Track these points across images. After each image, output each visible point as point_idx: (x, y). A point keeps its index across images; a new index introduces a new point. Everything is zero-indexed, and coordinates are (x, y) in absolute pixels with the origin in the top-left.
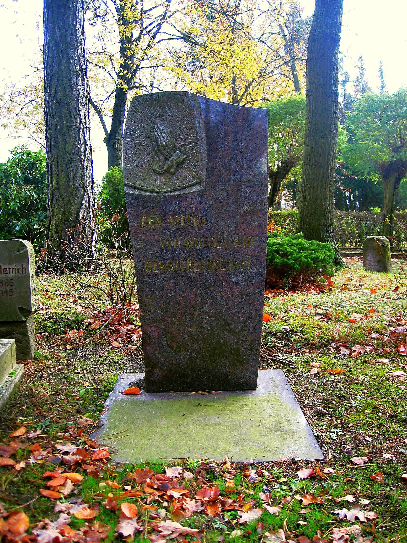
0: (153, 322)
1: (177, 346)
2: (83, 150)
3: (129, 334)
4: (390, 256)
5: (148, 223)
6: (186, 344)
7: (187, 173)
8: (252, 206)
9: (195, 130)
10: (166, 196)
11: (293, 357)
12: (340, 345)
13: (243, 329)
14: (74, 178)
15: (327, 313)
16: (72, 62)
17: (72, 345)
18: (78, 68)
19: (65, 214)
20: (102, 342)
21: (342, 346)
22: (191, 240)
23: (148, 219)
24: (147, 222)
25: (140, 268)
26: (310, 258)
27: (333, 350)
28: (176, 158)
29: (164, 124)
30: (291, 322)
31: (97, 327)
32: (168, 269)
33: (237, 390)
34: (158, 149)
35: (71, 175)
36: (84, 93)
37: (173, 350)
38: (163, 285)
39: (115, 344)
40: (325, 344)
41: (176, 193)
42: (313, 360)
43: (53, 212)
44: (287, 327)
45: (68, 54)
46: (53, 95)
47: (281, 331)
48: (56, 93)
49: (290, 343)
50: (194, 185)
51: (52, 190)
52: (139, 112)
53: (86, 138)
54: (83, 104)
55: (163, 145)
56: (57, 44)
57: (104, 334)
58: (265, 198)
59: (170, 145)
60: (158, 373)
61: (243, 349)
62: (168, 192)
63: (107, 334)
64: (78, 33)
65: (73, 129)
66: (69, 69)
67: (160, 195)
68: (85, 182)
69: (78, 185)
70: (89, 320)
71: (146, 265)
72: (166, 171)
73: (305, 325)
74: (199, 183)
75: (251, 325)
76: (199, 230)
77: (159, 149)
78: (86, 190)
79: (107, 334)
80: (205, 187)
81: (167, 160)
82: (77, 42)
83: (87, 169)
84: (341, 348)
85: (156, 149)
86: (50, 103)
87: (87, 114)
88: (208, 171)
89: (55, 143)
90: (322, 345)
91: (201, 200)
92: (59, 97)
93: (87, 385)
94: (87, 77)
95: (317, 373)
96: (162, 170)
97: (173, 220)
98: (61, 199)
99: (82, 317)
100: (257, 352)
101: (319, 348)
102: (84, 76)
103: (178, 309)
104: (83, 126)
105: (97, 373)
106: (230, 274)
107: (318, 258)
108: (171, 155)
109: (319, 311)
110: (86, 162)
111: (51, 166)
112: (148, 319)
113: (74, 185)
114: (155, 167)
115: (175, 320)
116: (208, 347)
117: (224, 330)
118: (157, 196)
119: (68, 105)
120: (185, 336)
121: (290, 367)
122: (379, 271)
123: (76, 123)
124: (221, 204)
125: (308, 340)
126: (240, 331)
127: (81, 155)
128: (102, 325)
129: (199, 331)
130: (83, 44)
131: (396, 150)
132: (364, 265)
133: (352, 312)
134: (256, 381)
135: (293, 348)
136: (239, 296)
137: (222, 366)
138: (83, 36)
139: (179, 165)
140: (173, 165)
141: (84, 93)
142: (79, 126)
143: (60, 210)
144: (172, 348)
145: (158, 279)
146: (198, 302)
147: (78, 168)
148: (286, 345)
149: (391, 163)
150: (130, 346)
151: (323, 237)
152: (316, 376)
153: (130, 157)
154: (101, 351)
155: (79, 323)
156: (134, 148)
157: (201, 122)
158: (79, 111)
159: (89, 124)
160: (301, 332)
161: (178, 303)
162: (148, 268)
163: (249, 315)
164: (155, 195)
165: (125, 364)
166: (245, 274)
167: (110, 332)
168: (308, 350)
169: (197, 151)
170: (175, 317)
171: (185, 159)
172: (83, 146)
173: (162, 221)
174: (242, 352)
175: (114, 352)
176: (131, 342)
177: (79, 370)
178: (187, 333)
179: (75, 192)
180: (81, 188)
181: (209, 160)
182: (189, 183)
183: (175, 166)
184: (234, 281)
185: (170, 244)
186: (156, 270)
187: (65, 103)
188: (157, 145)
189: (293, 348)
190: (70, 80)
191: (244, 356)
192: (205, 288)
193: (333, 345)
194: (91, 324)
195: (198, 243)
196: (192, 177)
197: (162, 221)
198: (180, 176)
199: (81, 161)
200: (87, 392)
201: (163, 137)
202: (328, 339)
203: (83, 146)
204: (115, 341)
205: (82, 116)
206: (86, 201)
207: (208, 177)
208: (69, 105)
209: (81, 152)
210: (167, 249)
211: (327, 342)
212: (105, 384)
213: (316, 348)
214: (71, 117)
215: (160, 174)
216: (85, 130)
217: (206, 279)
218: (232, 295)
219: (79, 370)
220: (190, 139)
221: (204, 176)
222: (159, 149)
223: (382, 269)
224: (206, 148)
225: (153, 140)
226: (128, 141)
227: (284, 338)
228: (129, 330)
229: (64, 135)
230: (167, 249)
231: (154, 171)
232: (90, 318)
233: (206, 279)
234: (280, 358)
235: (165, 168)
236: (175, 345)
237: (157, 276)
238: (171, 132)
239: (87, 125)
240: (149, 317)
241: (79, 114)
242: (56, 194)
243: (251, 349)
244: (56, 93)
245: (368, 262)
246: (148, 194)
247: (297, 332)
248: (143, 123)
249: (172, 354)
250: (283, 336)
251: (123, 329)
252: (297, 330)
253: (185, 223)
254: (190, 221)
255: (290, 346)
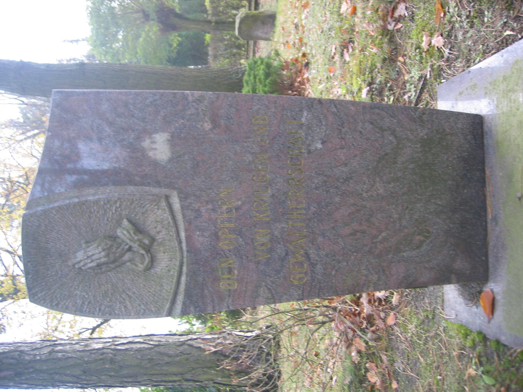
0: (384, 271)
1: (419, 234)
2: (139, 346)
3: (375, 301)
4: (257, 12)
5: (229, 279)
6: (417, 220)
7: (152, 218)
8: (204, 115)
9: (84, 204)
10: (188, 251)
11: (412, 77)
12: (392, 17)
13: (393, 133)
14: (170, 356)
15: (340, 46)
16: (38, 358)
17: (390, 379)
18: (46, 351)
19: (211, 367)
20: (386, 339)
21: (393, 14)
22: (257, 212)
23: (223, 279)
24: (228, 282)
25: (300, 292)
26: (265, 82)
27: (399, 26)
28: (128, 235)
29: (75, 253)
30: (355, 88)
31: (364, 344)
32: (302, 248)
33: (483, 143)
34: (114, 262)
35: (166, 359)
36: (75, 344)
37: (424, 241)
38: (327, 255)
39: (391, 321)
40: (391, 38)
41: (183, 235)
42: (419, 47)
43: (208, 380)
44: (365, 91)
45: (30, 362)
46: (75, 380)
47: (371, 97)
48: (74, 376)
49: (389, 85)
50: (170, 206)
51: (183, 381)
52: (54, 292)
53: (125, 342)
54: (86, 346)
55: (107, 255)
56: (18, 374)
57: (375, 336)
58: (192, 95)
59: (106, 244)
60: (460, 264)
61: (423, 133)
62: (181, 249)
63: (373, 332)
64: (6, 350)
65: (115, 357)
66: (46, 361)
67: (185, 260)
68: (174, 343)
69: (178, 352)
70: (353, 354)
71: (296, 283)
72: (148, 249)
73: (360, 69)
74: (167, 198)
75: (387, 120)
76: (239, 200)
77: (114, 262)
78: (183, 343)
79: (373, 332)
80: (174, 188)
81: (130, 249)
82: (16, 351)
83: (160, 341)
84: (396, 15)
85: (112, 266)
86: (85, 382)
87: (98, 340)
88: (149, 184)
89: (130, 377)
90: (391, 41)
91: (195, 196)
92: (78, 372)
93: (471, 371)
94: (56, 341)
95: (442, 35)
96: (146, 256)
97: (226, 239)
98: (193, 372)
99: (348, 363)
100: (427, 112)
101: (397, 45)
102: (55, 344)
103: (364, 232)
104: (111, 345)
105: (444, 351)
106: (309, 152)
107: (265, 72)
108: (123, 241)
109: (337, 57)
110: (152, 343)
111: (156, 382)
112: (379, 279)
113: (177, 356)
114: (141, 267)
115: (380, 237)
116: (420, 186)
117: (395, 163)
118: (188, 266)
119: (87, 363)
120: (404, 223)
121: (430, 78)
122: (273, 25)
123: (107, 353)
124: (201, 164)
125: (385, 60)
126: (396, 137)
127: (144, 348)
128: (361, 337)
129: (397, 201)
130: (20, 344)
131: (146, 17)
132: (267, 39)
133: (340, 15)
134: (468, 115)
135: (396, 80)
136: (343, 139)
137: (448, 166)
138: (10, 344)
139: (138, 229)
140: (139, 240)
141: (75, 344)
142: (112, 350)
143: (205, 373)
144: (422, 243)
145: (316, 264)
146: (352, 201)
147: (159, 352)
148: (391, 89)
149: (161, 22)
150: (395, 300)
151: (238, 79)
152: (449, 36)
153: (125, 307)
154: (401, 342)
155: (357, 367)
156: (111, 301)
157: (72, 194)
158: (94, 349)
159: (109, 338)
160: (371, 72)
161: (354, 233)
162: (300, 279)
163: (372, 123)
164: (185, 269)
165: (427, 311)
166: (309, 128)
167: (371, 326)
168: (401, 59)
169: (116, 202)
170: (376, 237)
171: (130, 221)
172: (134, 346)
173: (227, 257)
174: (427, 134)
175: (406, 325)
176: (387, 300)
177: (439, 377)
178: (400, 219)
179: (186, 356)
180: (181, 349)
181: (131, 182)
182: (167, 215)
183: (140, 237)
184: (319, 146)
185: (262, 245)
186: (303, 265)
187: (85, 365)
188: (107, 263)
189: (396, 80)
190: (60, 359)
191: (433, 132)
192: (331, 190)
193: (390, 27)
194: (359, 352)
195: (262, 200)
196: (158, 209)
197: (227, 257)
198: (156, 228)
199: (151, 348)
200: (486, 372)
201: (93, 255)
202: (382, 35)
203: (134, 346)
204: (384, 320)
205: (100, 346)
206: (196, 342)
207: (158, 184)
208: (87, 361)
209: (140, 348)
210: (271, 250)
211: (387, 35)
212: (469, 343)
213: (396, 48)
214: (101, 359)
215: (153, 260)
216: (117, 343)
217: (317, 188)
218: (342, 148)
219: (439, 377)
220: (98, 212)
221: (156, 190)
222: (114, 262)
223: (271, 20)
224: (112, 187)
225: (99, 271)
226: (100, 309)
227: (381, 93)
228: (369, 302)
229: (121, 367)
230: (271, 250)
231: (148, 269)
232: (350, 353)
233: (317, 188)
234: (414, 94)
235: (143, 252)
236: (418, 237)
237: (313, 265)
238: (87, 242)
239: (110, 340)
240: (375, 278)
241: (98, 349)
242: (188, 376)
243: (422, 121)
244: (74, 376)
245: (264, 36)
246: (183, 279)
247: (372, 77)
248: (71, 287)
249: (431, 242)
250: (377, 95)
251: (367, 309)
252: (368, 77)
253: (229, 221)
254: (227, 213)
255: (397, 83)
